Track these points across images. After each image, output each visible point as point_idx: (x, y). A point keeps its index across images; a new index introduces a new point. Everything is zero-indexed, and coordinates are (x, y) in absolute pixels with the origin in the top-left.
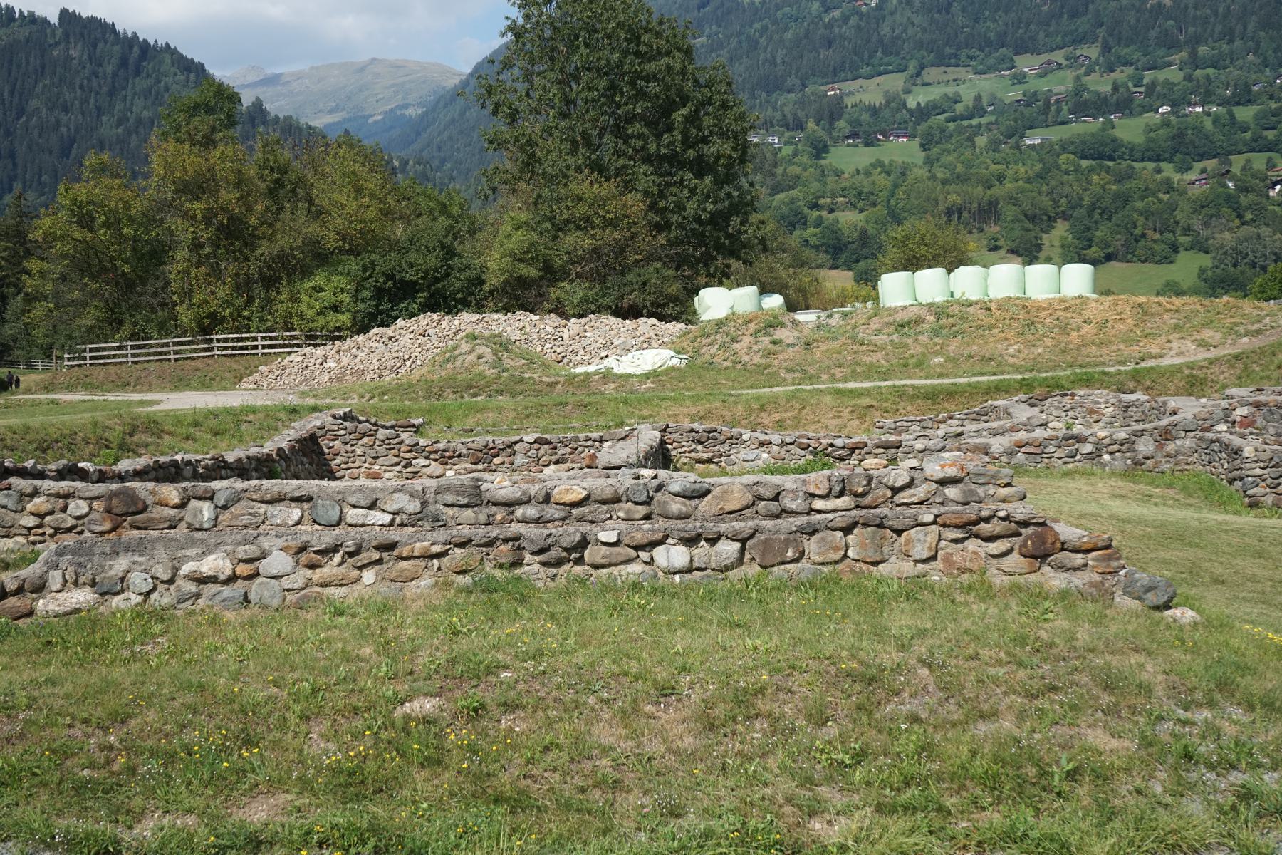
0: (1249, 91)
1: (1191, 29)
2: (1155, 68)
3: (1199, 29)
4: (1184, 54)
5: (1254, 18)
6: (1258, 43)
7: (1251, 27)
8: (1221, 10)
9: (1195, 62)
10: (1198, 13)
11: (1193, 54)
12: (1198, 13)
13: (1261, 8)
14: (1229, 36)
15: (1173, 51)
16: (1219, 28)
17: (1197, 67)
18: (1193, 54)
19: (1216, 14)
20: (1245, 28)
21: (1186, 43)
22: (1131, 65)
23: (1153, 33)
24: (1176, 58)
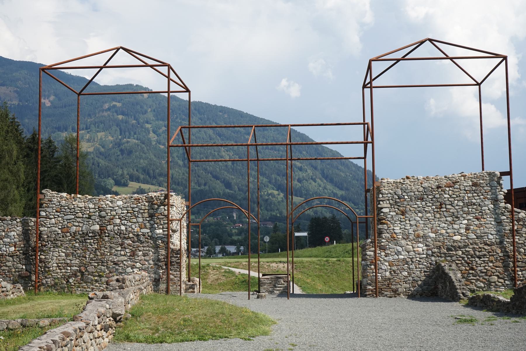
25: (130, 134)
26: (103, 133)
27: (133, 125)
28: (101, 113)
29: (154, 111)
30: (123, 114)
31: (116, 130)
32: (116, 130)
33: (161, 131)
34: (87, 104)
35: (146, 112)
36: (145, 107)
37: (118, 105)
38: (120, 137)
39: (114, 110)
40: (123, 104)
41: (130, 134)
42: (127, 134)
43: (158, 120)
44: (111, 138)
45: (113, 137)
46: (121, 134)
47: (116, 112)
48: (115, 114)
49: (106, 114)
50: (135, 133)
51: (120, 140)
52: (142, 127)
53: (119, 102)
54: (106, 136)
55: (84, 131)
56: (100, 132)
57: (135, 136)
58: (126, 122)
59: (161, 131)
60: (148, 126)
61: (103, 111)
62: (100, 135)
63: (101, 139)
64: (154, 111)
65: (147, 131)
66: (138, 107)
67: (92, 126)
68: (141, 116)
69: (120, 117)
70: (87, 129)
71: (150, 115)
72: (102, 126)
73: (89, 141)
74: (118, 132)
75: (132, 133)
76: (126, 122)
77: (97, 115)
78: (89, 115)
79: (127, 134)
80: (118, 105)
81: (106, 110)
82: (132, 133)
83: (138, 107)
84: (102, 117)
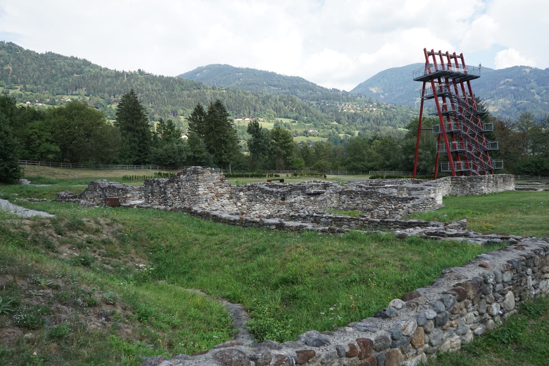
0: (55, 101)
1: (22, 79)
2: (11, 89)
3: (25, 80)
4: (22, 86)
5: (43, 80)
6: (46, 87)
7: (42, 82)
8: (31, 75)
9: (26, 89)
10: (24, 75)
11: (25, 87)
12: (24, 75)
13: (45, 77)
14: (35, 83)
15: (16, 85)
16: (31, 80)
17: (26, 91)
18: (25, 87)
19: (30, 76)
20: (40, 82)
21: (21, 83)
22: (2, 86)
23: (9, 78)
24: (19, 87)
25: (521, 97)
26: (503, 99)
27: (522, 92)
28: (499, 87)
29: (536, 80)
30: (514, 85)
31: (511, 96)
32: (511, 96)
33: (543, 93)
34: (489, 83)
35: (530, 82)
36: (529, 79)
37: (510, 80)
38: (514, 100)
39: (508, 84)
40: (514, 79)
41: (521, 97)
42: (519, 98)
43: (539, 85)
44: (508, 102)
45: (510, 101)
46: (515, 99)
47: (510, 85)
48: (509, 86)
49: (503, 87)
50: (525, 97)
51: (515, 102)
52: (529, 92)
53: (510, 78)
54: (505, 101)
55: (489, 100)
56: (500, 99)
57: (525, 98)
58: (518, 90)
59: (543, 93)
60: (532, 91)
61: (500, 85)
62: (501, 100)
63: (502, 103)
64: (536, 80)
65: (533, 94)
66: (525, 80)
67: (495, 96)
68: (528, 85)
69: (513, 88)
70: (491, 98)
71: (534, 84)
72: (501, 95)
73: (494, 105)
74: (513, 97)
75: (523, 97)
76: (518, 90)
77: (497, 89)
78: (492, 89)
79: (519, 98)
80: (510, 80)
81: (502, 85)
82: (523, 97)
83: (525, 80)
84: (501, 89)
